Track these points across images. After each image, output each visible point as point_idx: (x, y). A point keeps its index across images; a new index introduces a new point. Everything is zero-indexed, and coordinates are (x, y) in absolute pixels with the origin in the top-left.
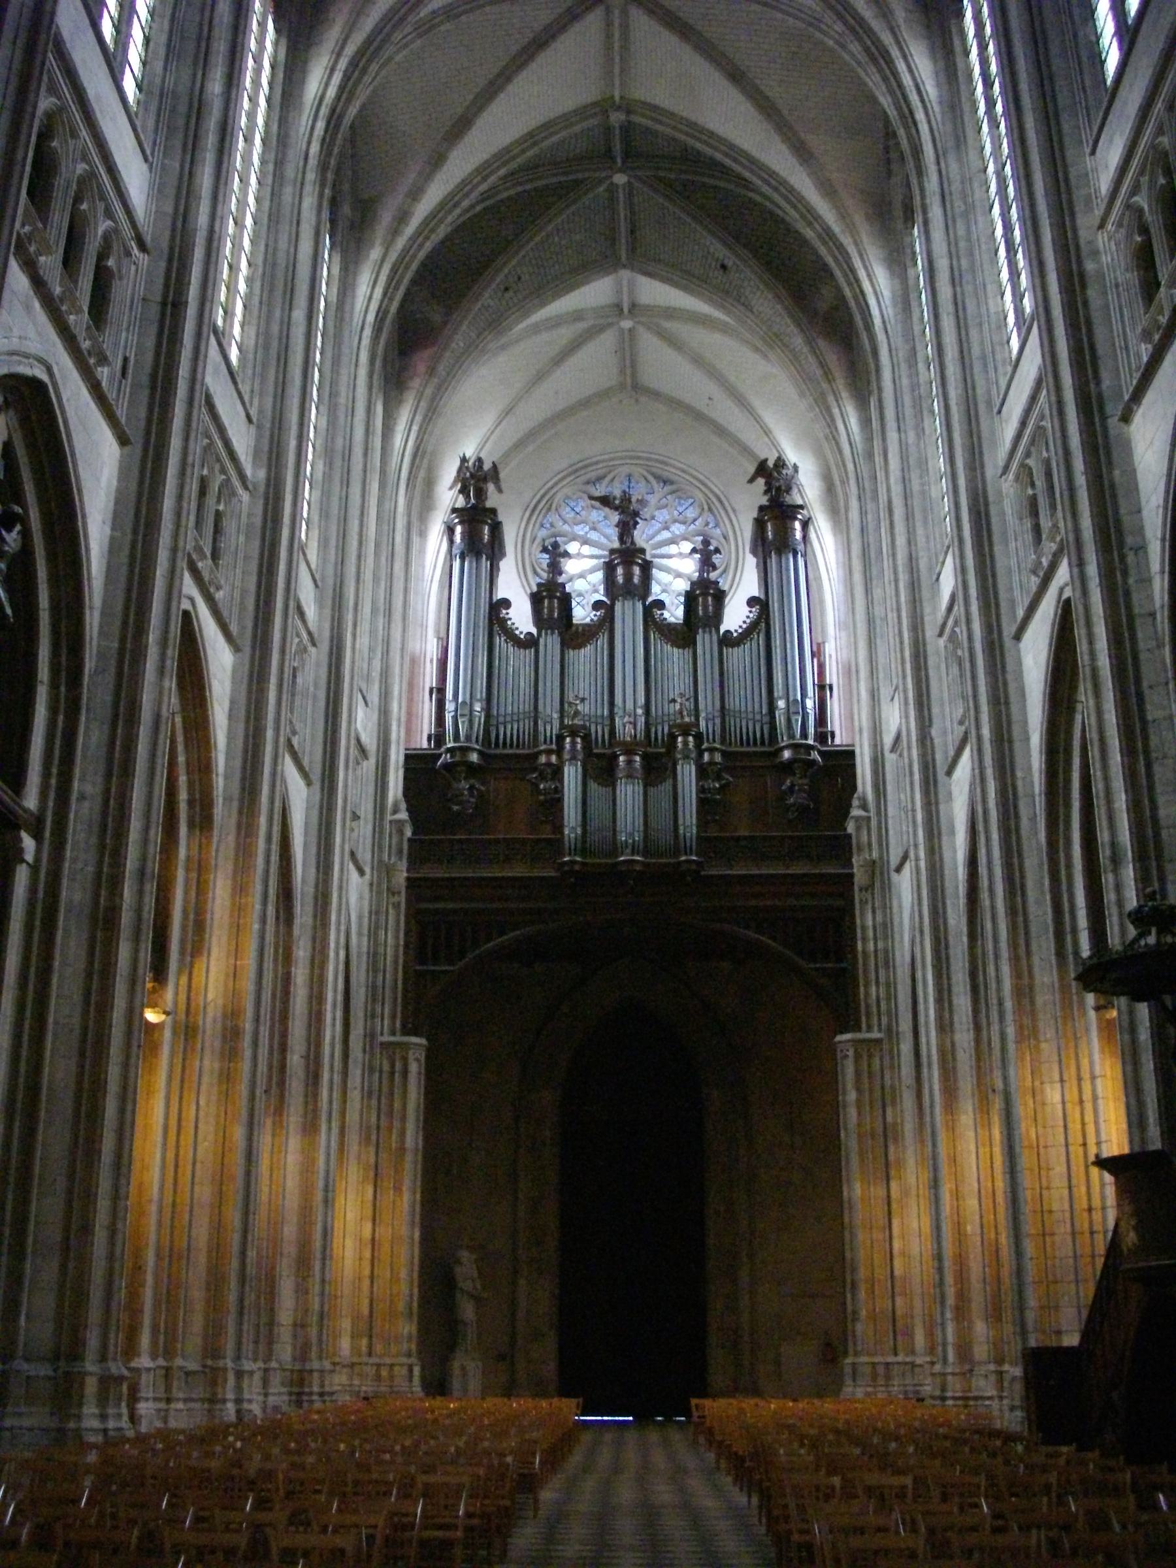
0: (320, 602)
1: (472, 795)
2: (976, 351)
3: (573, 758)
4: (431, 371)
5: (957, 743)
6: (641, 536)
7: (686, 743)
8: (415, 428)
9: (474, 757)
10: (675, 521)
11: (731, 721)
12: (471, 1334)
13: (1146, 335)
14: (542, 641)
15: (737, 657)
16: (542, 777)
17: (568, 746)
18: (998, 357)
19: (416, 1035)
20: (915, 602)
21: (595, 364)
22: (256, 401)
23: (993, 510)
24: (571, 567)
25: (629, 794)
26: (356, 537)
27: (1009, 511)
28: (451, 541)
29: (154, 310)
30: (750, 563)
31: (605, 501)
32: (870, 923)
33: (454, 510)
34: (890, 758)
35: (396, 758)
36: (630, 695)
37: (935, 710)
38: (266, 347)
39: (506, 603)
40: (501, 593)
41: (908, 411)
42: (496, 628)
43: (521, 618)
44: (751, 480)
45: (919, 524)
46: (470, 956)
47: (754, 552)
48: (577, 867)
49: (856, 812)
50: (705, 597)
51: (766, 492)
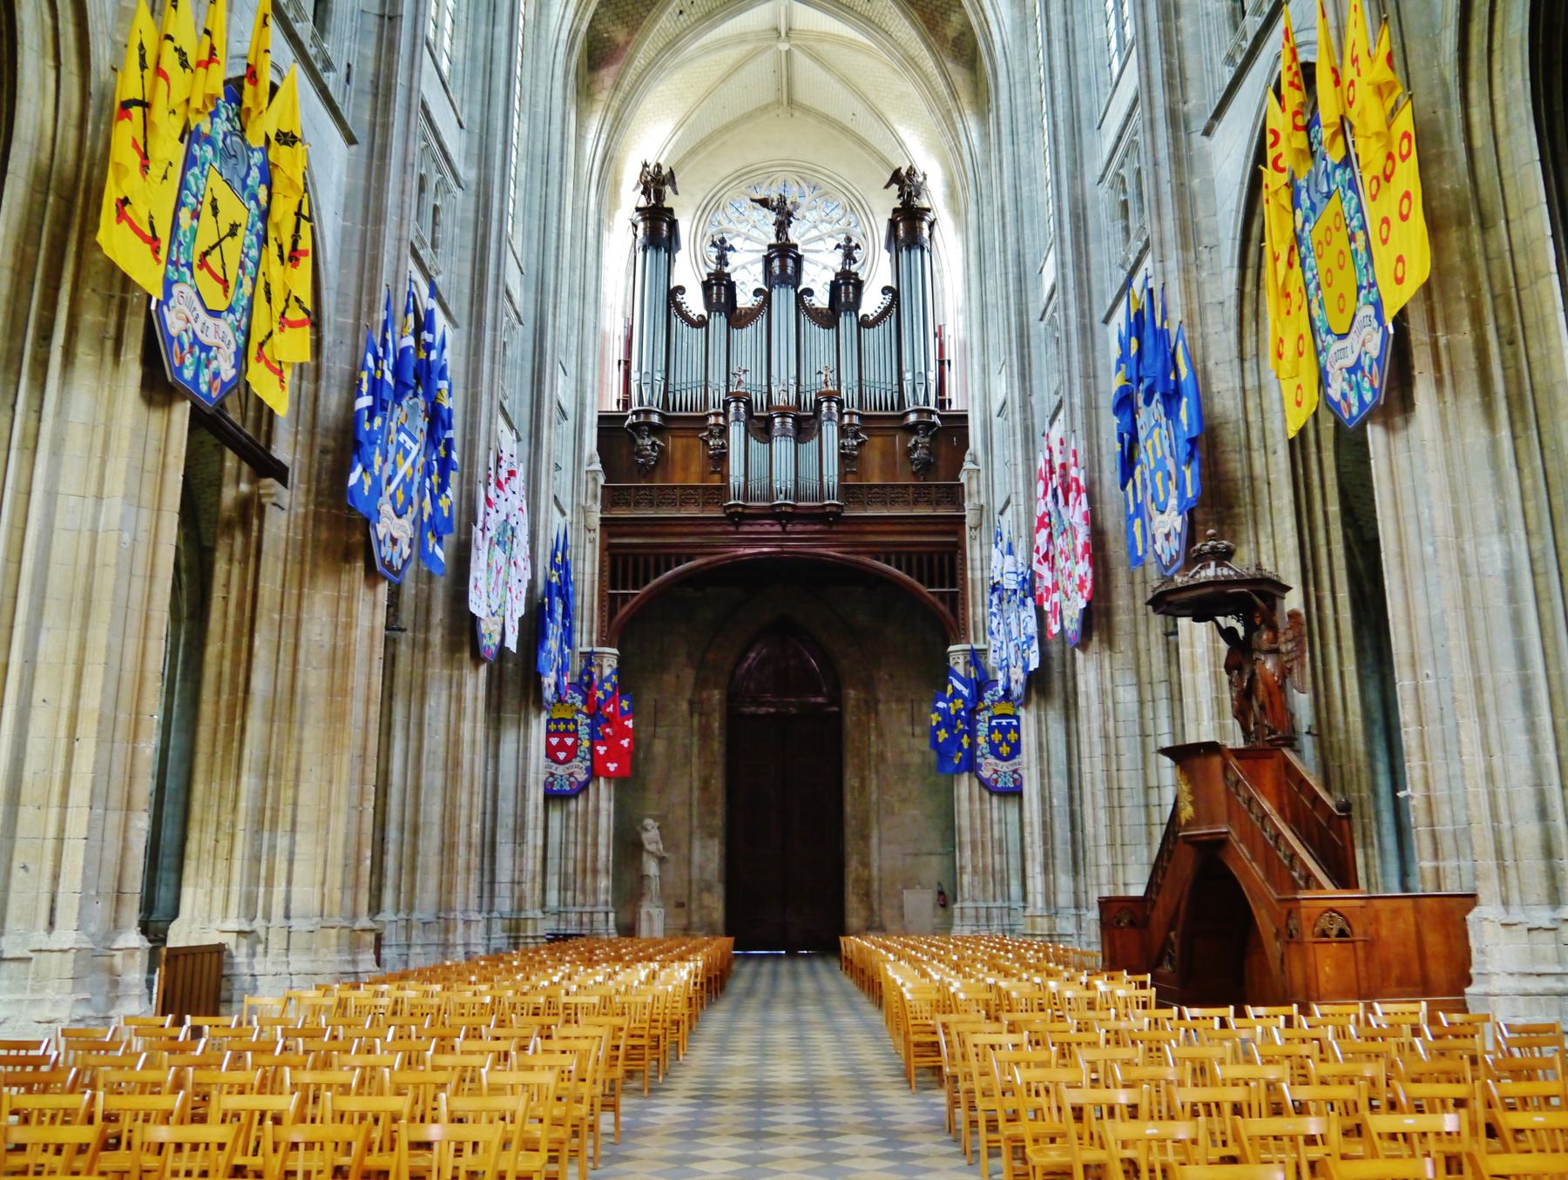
2: (1081, 72)
4: (616, 86)
7: (829, 408)
8: (604, 136)
11: (866, 391)
12: (654, 885)
13: (1230, 59)
16: (711, 435)
18: (1101, 79)
19: (610, 646)
20: (1021, 291)
21: (758, 82)
22: (466, 109)
25: (783, 447)
27: (1103, 215)
29: (372, 23)
30: (885, 257)
31: (764, 203)
32: (977, 555)
33: (638, 209)
34: (997, 422)
37: (1035, 382)
38: (474, 59)
39: (681, 289)
41: (1022, 128)
42: (673, 310)
43: (694, 302)
44: (887, 187)
46: (654, 582)
47: (888, 248)
49: (967, 465)
50: (847, 286)
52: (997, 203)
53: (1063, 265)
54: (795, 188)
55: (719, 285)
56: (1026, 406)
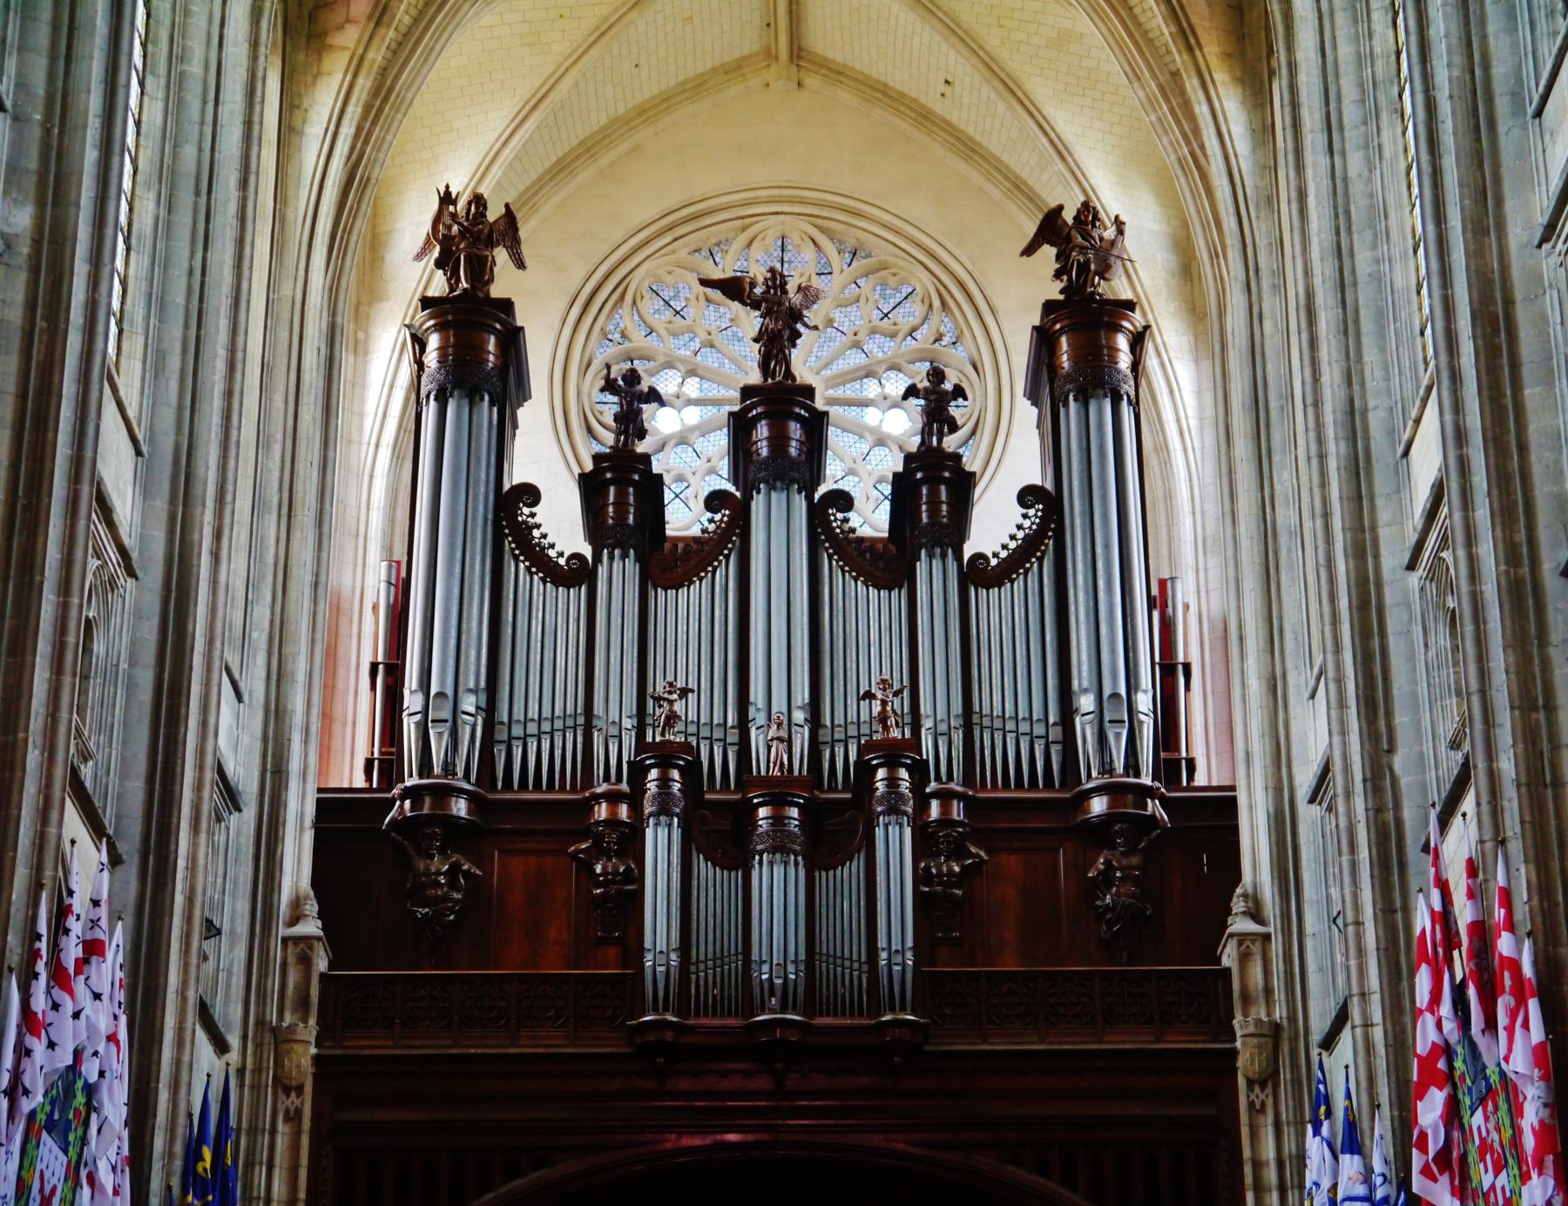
0: (145, 487)
1: (453, 884)
3: (664, 809)
5: (1447, 787)
6: (805, 362)
7: (892, 781)
8: (347, 131)
9: (460, 807)
10: (874, 331)
14: (602, 571)
15: (998, 609)
16: (599, 851)
17: (652, 787)
23: (1522, 314)
24: (661, 421)
25: (776, 883)
26: (222, 353)
28: (420, 365)
30: (1026, 415)
31: (733, 288)
33: (426, 302)
34: (1309, 815)
35: (300, 807)
36: (779, 684)
37: (1401, 719)
39: (530, 494)
40: (520, 472)
41: (1351, 113)
43: (561, 524)
44: (1029, 251)
45: (1368, 341)
47: (1033, 396)
48: (669, 1036)
49: (1240, 924)
50: (934, 485)
51: (1058, 275)
52: (1296, 288)
53: (1461, 437)
54: (809, 253)
55: (622, 483)
56: (1379, 775)
